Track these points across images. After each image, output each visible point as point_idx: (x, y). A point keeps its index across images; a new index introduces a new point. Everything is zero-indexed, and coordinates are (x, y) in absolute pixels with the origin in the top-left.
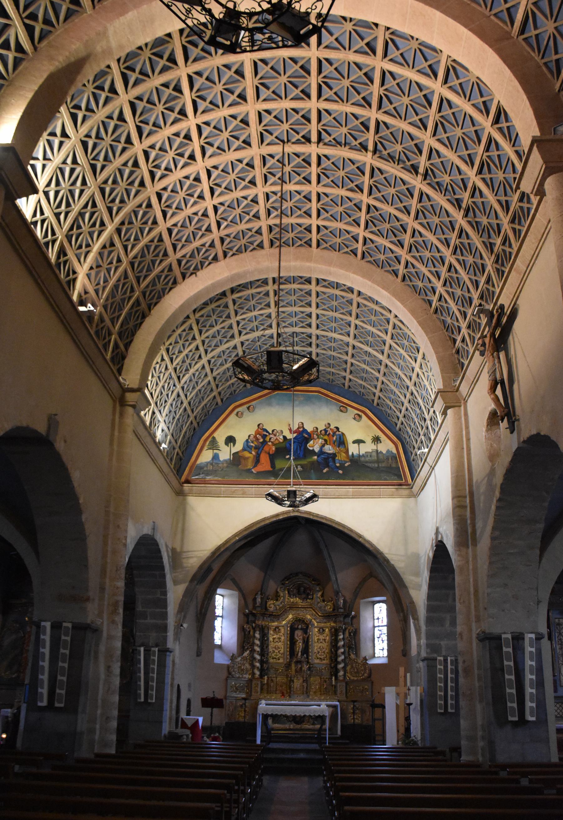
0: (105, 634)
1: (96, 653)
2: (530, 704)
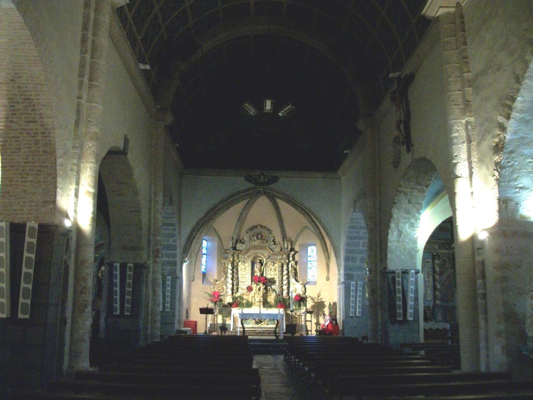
0: (151, 270)
1: (147, 282)
2: (410, 311)
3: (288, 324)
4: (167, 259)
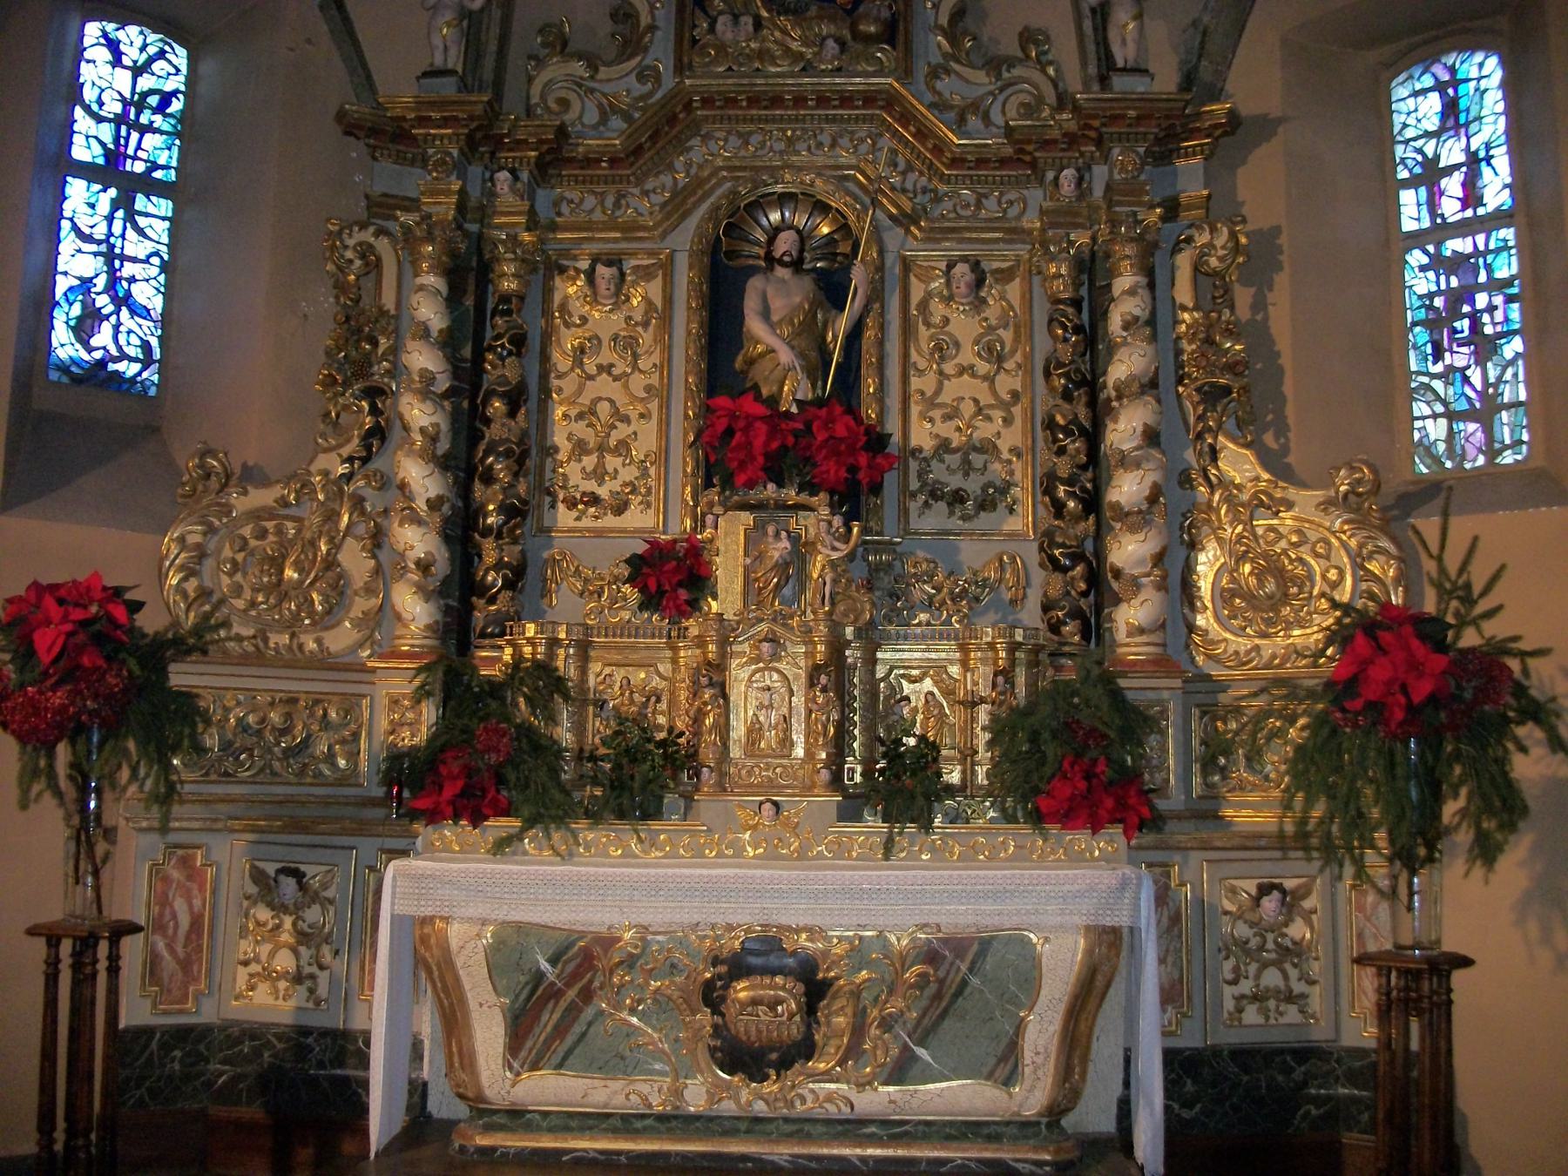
3: (1190, 1039)
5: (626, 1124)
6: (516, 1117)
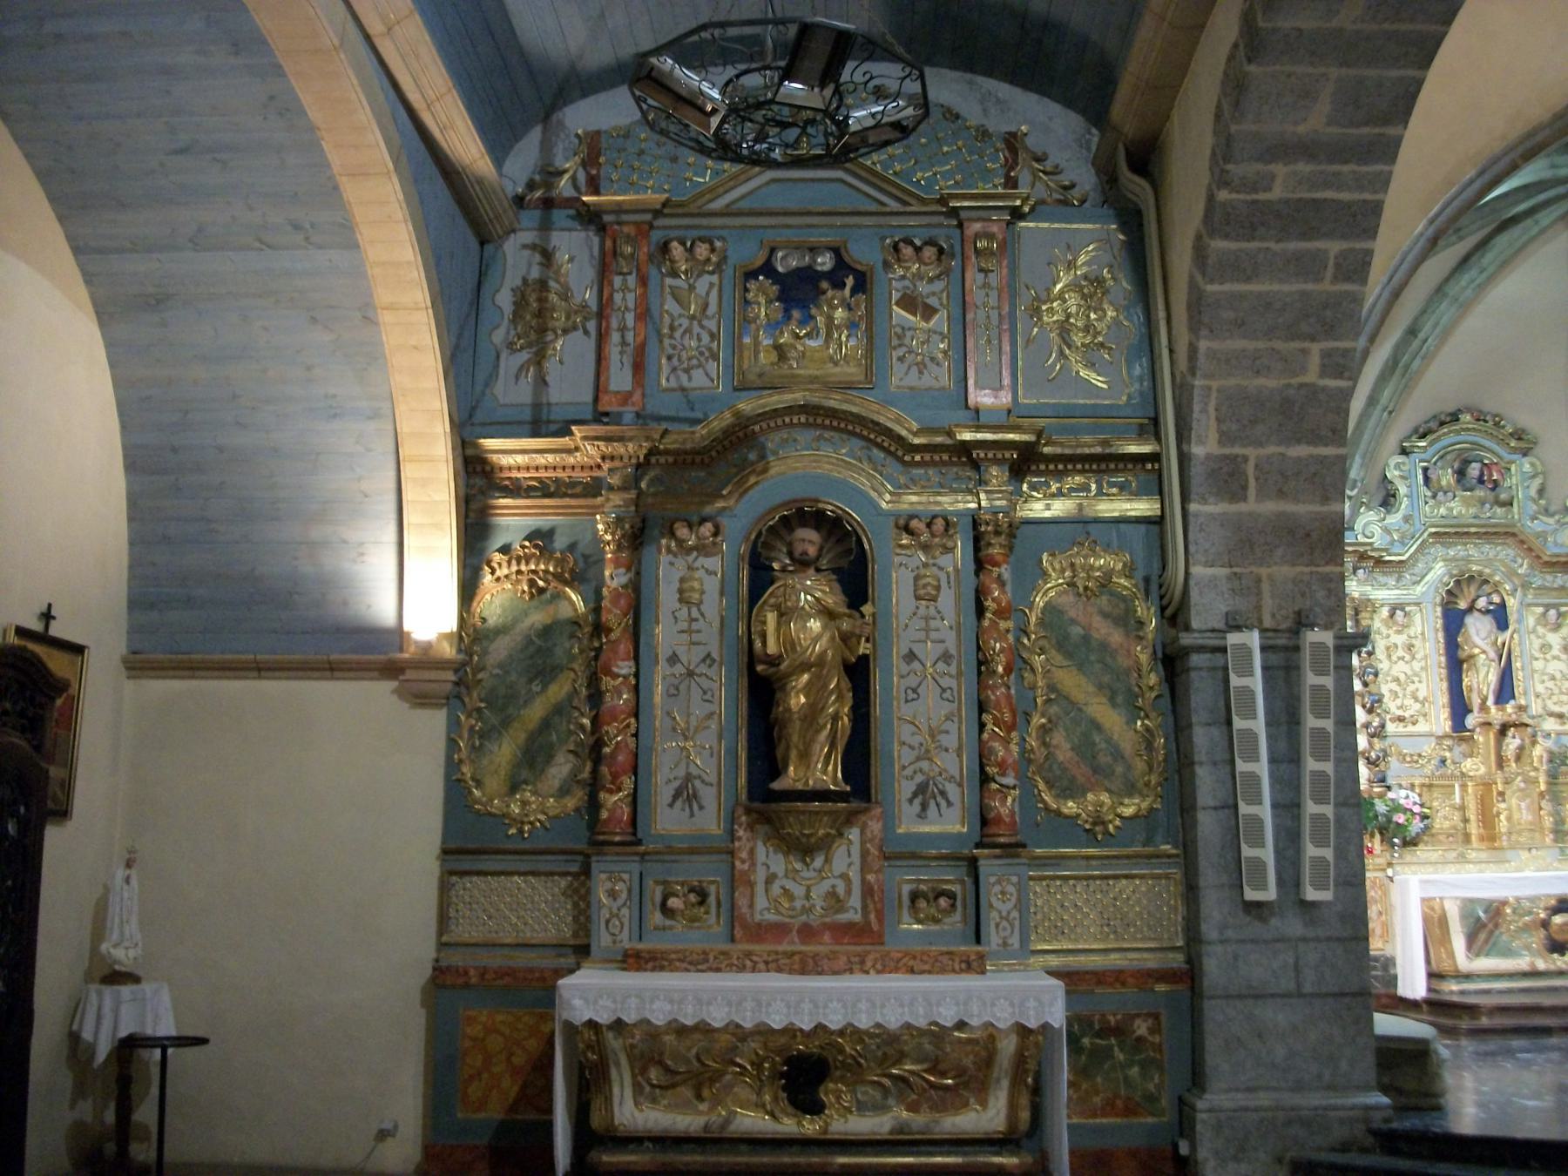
4: (1270, 507)
5: (1511, 976)
6: (1468, 977)
